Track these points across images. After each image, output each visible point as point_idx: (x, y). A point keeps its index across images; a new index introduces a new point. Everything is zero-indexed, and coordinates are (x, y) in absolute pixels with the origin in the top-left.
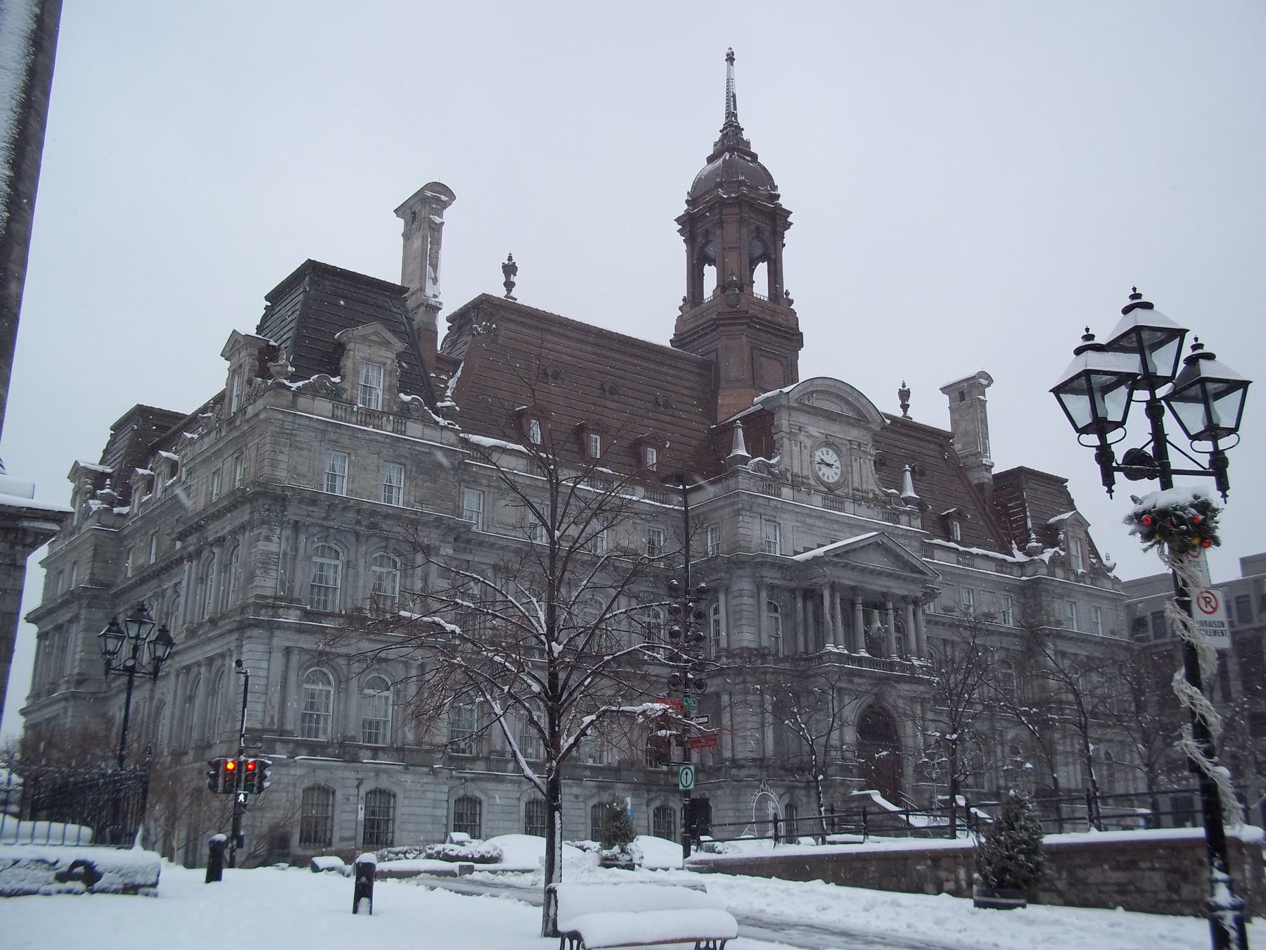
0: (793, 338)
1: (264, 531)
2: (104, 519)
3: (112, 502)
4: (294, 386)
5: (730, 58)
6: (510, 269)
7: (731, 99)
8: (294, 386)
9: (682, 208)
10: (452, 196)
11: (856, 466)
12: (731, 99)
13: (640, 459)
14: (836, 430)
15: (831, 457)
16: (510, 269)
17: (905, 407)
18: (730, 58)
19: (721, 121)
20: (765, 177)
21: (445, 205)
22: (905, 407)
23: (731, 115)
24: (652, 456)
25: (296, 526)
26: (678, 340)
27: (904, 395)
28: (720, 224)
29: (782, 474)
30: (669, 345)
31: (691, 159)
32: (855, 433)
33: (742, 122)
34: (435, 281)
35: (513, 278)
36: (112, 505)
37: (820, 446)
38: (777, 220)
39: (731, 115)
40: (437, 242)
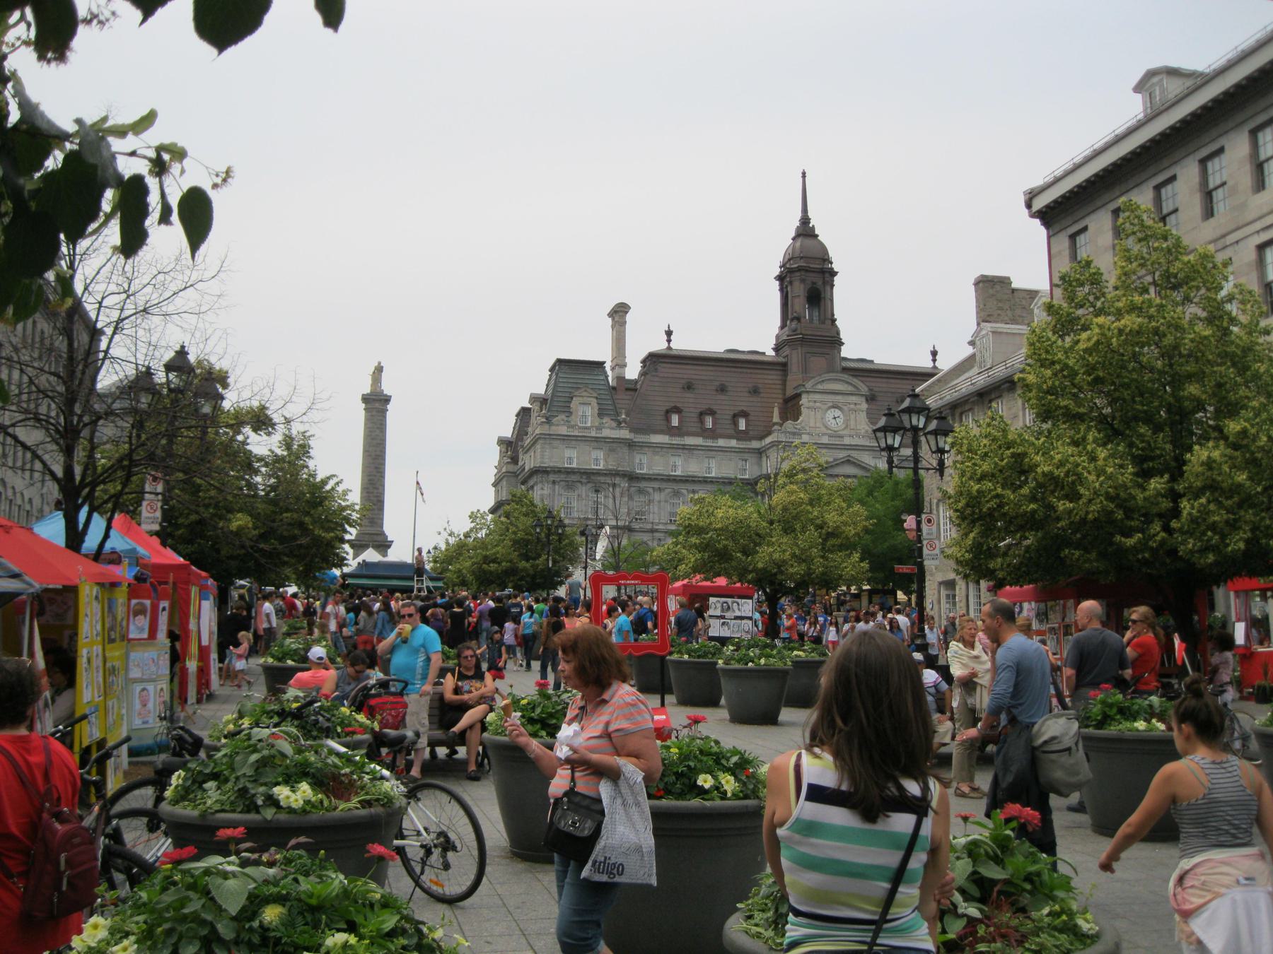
0: (836, 342)
5: (804, 175)
6: (669, 333)
9: (777, 271)
11: (852, 417)
13: (736, 424)
14: (839, 398)
15: (837, 413)
16: (669, 333)
17: (934, 361)
18: (804, 175)
19: (799, 215)
22: (934, 361)
24: (742, 424)
25: (554, 482)
26: (777, 349)
27: (934, 353)
28: (791, 283)
30: (771, 353)
32: (854, 399)
33: (810, 214)
37: (830, 408)
38: (829, 274)
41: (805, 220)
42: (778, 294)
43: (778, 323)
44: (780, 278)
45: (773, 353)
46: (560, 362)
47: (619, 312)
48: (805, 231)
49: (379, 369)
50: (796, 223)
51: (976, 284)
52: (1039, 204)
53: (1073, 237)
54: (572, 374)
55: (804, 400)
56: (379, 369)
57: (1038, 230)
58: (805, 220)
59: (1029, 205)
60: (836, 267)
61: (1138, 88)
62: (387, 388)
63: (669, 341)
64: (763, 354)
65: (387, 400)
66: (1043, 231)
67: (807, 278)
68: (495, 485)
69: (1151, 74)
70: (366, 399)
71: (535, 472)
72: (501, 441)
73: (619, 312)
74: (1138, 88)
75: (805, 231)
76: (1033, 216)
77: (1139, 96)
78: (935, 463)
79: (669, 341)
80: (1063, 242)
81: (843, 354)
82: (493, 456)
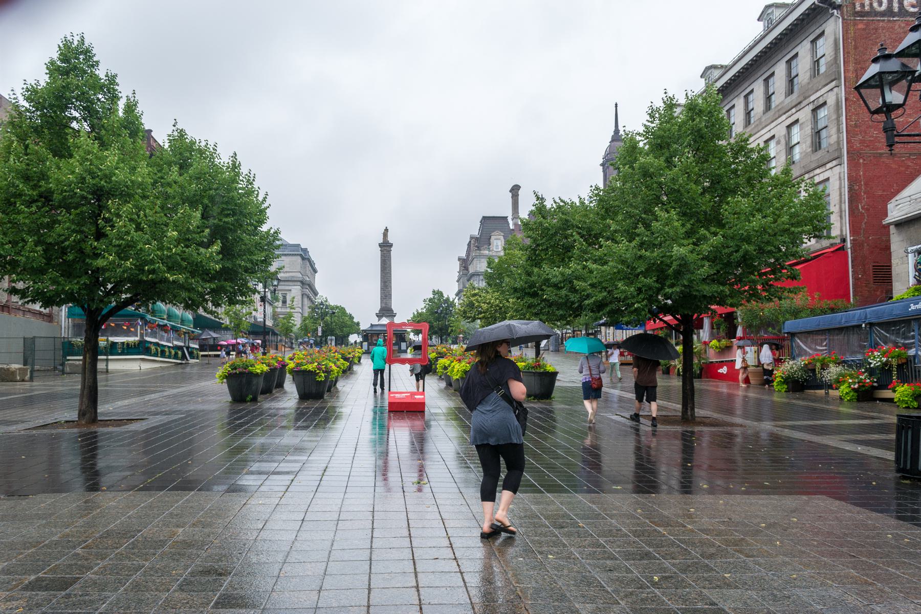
9: (601, 161)
41: (617, 131)
42: (602, 174)
44: (603, 165)
46: (484, 218)
47: (515, 190)
49: (386, 230)
54: (490, 223)
56: (386, 230)
62: (390, 239)
65: (391, 245)
68: (458, 281)
70: (380, 245)
71: (473, 275)
72: (459, 259)
73: (515, 190)
82: (457, 266)
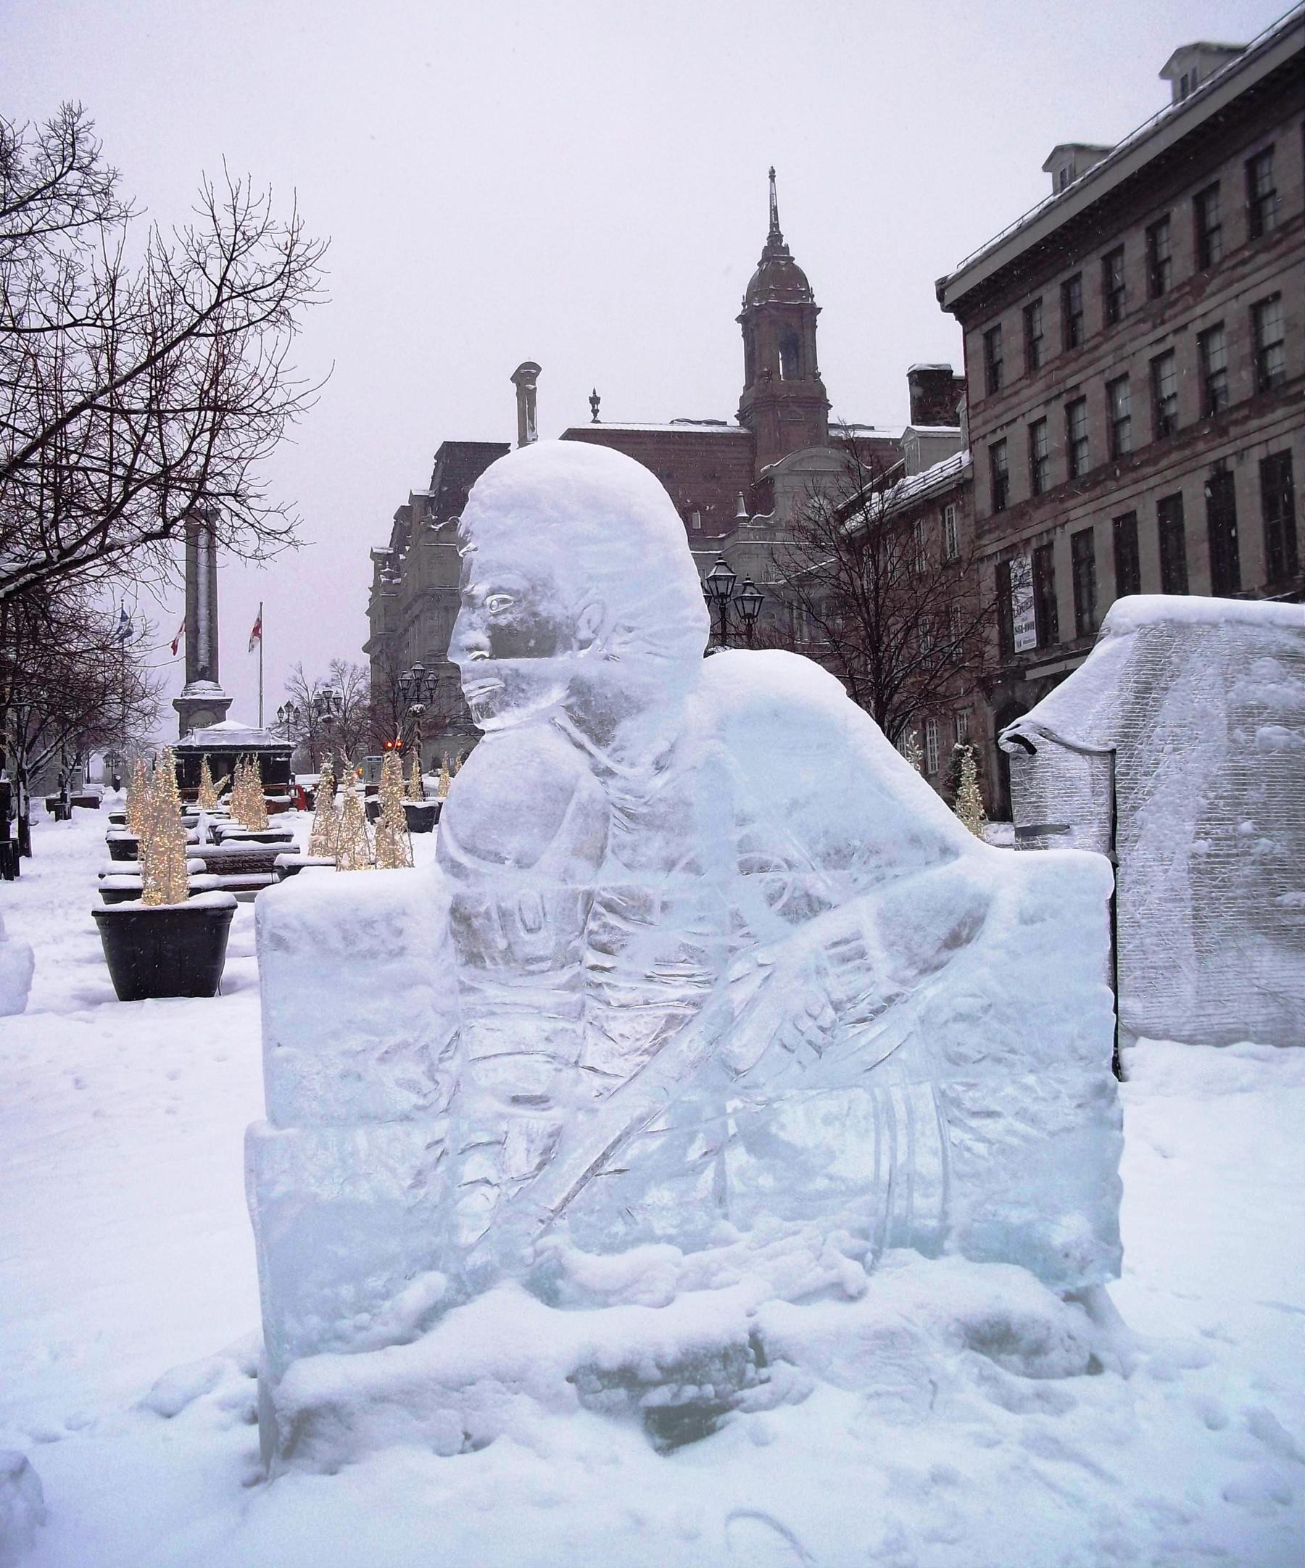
0: (820, 402)
1: (429, 614)
2: (389, 588)
3: (391, 576)
4: (437, 527)
5: (772, 176)
6: (595, 400)
7: (774, 210)
8: (437, 527)
9: (739, 310)
10: (539, 369)
12: (774, 210)
16: (595, 400)
18: (772, 176)
20: (798, 277)
21: (537, 375)
23: (774, 225)
28: (757, 325)
29: (778, 523)
31: (748, 265)
34: (533, 429)
35: (600, 407)
36: (392, 578)
39: (774, 225)
40: (532, 403)
41: (775, 236)
43: (741, 380)
45: (737, 423)
47: (526, 376)
48: (775, 252)
50: (761, 241)
51: (910, 375)
52: (951, 296)
53: (989, 337)
55: (778, 486)
57: (951, 327)
58: (775, 236)
59: (940, 297)
60: (818, 301)
61: (1046, 168)
63: (595, 412)
64: (724, 424)
66: (959, 327)
67: (780, 314)
69: (1059, 150)
72: (374, 555)
73: (526, 376)
74: (1046, 168)
75: (775, 252)
76: (946, 309)
77: (1050, 175)
78: (743, 628)
79: (595, 412)
80: (978, 341)
81: (832, 419)
82: (366, 573)
